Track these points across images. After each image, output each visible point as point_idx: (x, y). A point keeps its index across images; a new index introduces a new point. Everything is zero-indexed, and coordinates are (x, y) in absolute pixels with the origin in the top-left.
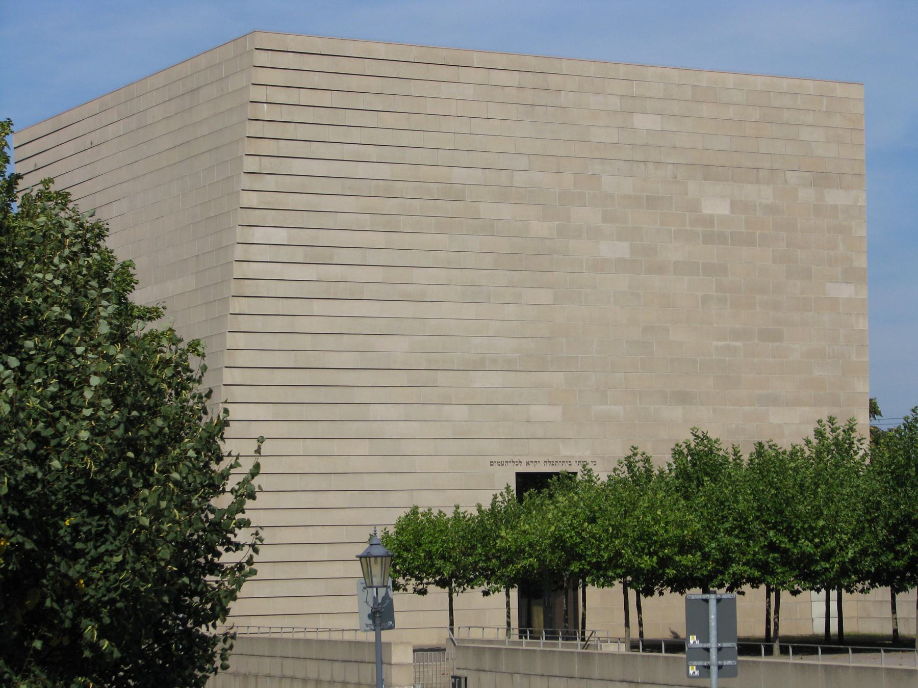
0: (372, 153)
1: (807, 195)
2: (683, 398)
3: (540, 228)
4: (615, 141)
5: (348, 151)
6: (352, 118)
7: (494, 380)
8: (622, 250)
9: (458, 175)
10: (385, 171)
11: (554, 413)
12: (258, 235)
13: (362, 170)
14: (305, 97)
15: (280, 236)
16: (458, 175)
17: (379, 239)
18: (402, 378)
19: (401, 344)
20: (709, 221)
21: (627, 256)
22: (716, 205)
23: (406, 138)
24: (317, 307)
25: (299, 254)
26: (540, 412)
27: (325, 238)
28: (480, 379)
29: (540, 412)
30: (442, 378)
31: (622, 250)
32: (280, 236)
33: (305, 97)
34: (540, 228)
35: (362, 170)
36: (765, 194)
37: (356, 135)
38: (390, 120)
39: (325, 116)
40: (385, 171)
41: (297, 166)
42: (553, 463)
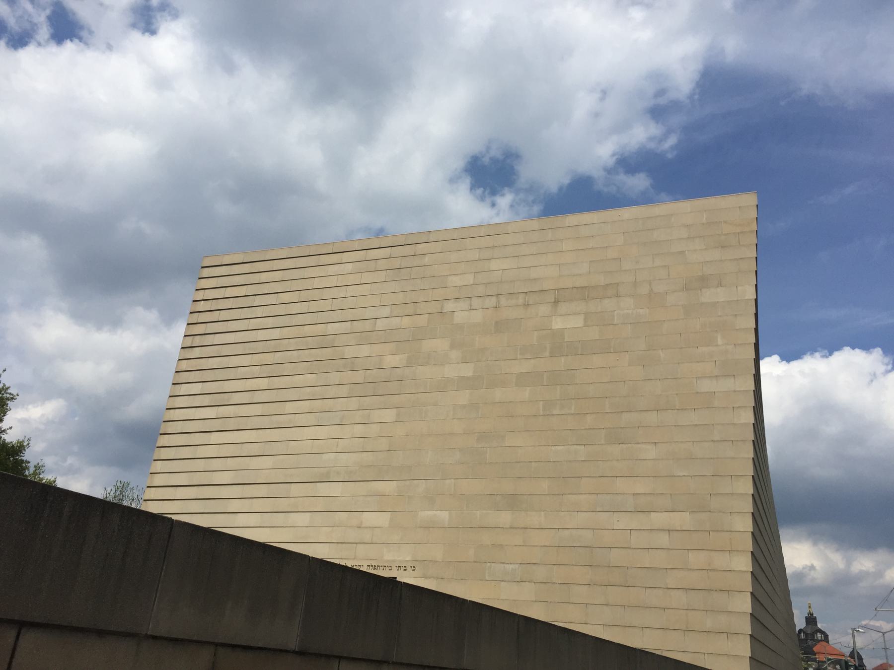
0: (269, 322)
3: (392, 360)
4: (471, 282)
5: (253, 324)
7: (336, 489)
9: (332, 328)
10: (276, 333)
11: (382, 519)
12: (183, 389)
14: (229, 292)
17: (263, 383)
18: (262, 491)
19: (267, 462)
21: (470, 374)
22: (568, 322)
24: (215, 438)
25: (206, 400)
26: (370, 519)
28: (324, 489)
29: (370, 519)
30: (295, 490)
31: (467, 370)
33: (229, 292)
37: (259, 312)
40: (276, 333)
42: (375, 568)
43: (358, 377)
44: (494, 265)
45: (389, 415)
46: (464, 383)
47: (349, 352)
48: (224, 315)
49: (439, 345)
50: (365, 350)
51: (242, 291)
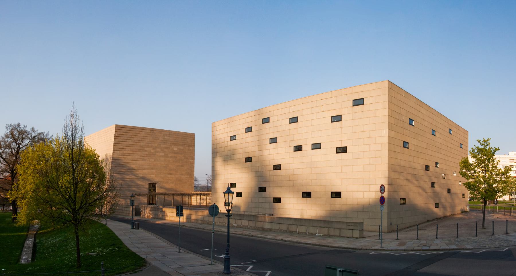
1: (187, 148)
2: (171, 174)
3: (152, 151)
6: (128, 136)
8: (163, 154)
9: (142, 144)
10: (132, 143)
12: (116, 152)
13: (129, 143)
14: (122, 133)
15: (118, 152)
16: (142, 144)
20: (175, 151)
22: (176, 149)
23: (135, 139)
27: (125, 152)
31: (163, 154)
32: (118, 152)
33: (122, 133)
34: (152, 151)
35: (129, 143)
36: (182, 148)
38: (133, 136)
39: (124, 136)
41: (121, 142)
43: (147, 153)
44: (166, 137)
45: (153, 160)
46: (163, 156)
47: (145, 149)
48: (122, 138)
49: (158, 149)
50: (148, 149)
51: (125, 134)
